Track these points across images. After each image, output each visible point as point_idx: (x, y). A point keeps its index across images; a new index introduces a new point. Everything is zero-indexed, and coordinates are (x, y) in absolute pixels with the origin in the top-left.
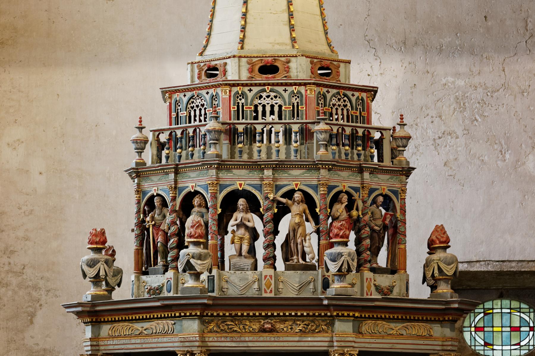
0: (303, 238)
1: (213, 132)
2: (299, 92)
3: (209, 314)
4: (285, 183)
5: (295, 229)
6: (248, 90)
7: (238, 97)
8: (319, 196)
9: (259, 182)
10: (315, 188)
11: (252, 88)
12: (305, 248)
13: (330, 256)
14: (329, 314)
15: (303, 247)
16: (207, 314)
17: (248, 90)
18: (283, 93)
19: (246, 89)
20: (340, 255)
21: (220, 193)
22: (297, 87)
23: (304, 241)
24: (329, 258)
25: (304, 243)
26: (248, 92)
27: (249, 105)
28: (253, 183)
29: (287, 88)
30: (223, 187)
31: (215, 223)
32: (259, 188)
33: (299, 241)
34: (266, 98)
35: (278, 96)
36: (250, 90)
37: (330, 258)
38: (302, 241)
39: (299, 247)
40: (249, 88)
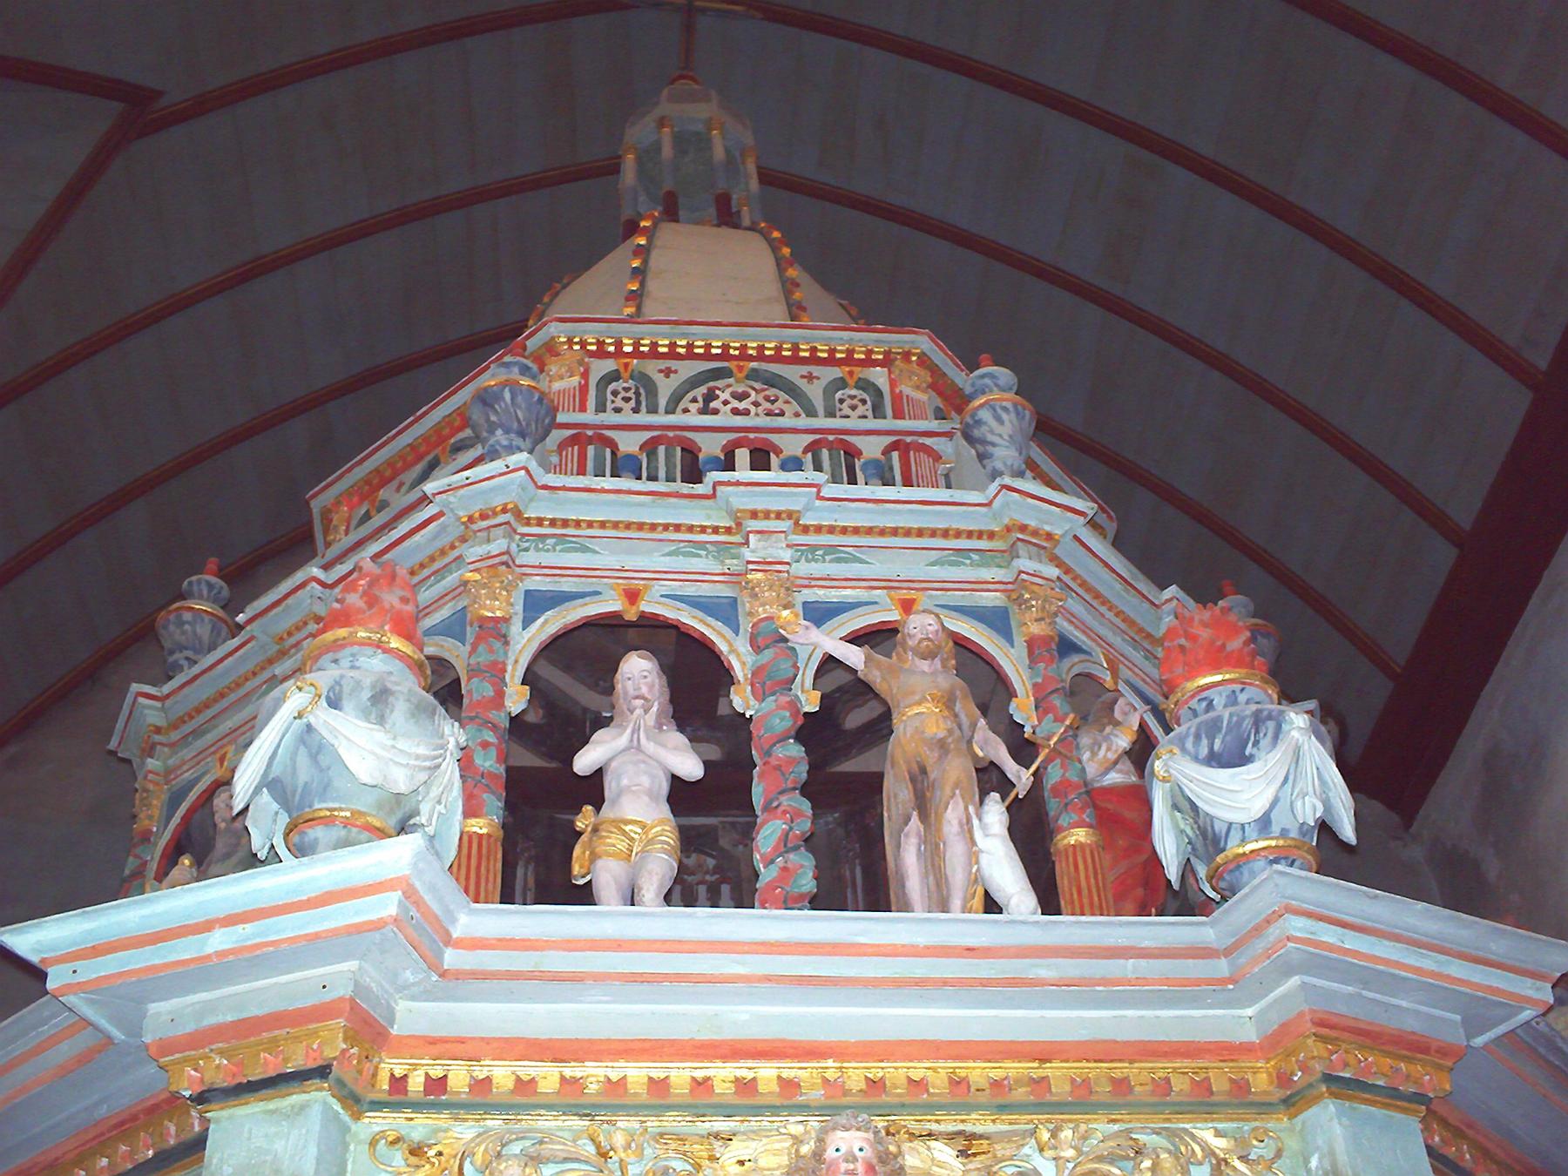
0: (971, 809)
1: (507, 395)
2: (865, 385)
3: (416, 1083)
4: (849, 594)
5: (923, 771)
6: (661, 371)
7: (615, 393)
8: (1020, 650)
9: (725, 591)
10: (997, 620)
11: (673, 364)
12: (984, 859)
13: (1205, 742)
14: (1261, 1081)
15: (973, 855)
16: (398, 1083)
17: (661, 371)
18: (803, 384)
19: (652, 368)
20: (1271, 725)
21: (526, 623)
22: (857, 369)
23: (975, 822)
24: (1196, 759)
25: (978, 835)
26: (659, 378)
27: (662, 407)
28: (690, 590)
29: (816, 370)
30: (536, 604)
31: (490, 737)
32: (725, 611)
33: (952, 816)
34: (731, 399)
35: (783, 396)
36: (668, 372)
37: (1204, 751)
38: (969, 820)
39: (955, 852)
40: (663, 364)
